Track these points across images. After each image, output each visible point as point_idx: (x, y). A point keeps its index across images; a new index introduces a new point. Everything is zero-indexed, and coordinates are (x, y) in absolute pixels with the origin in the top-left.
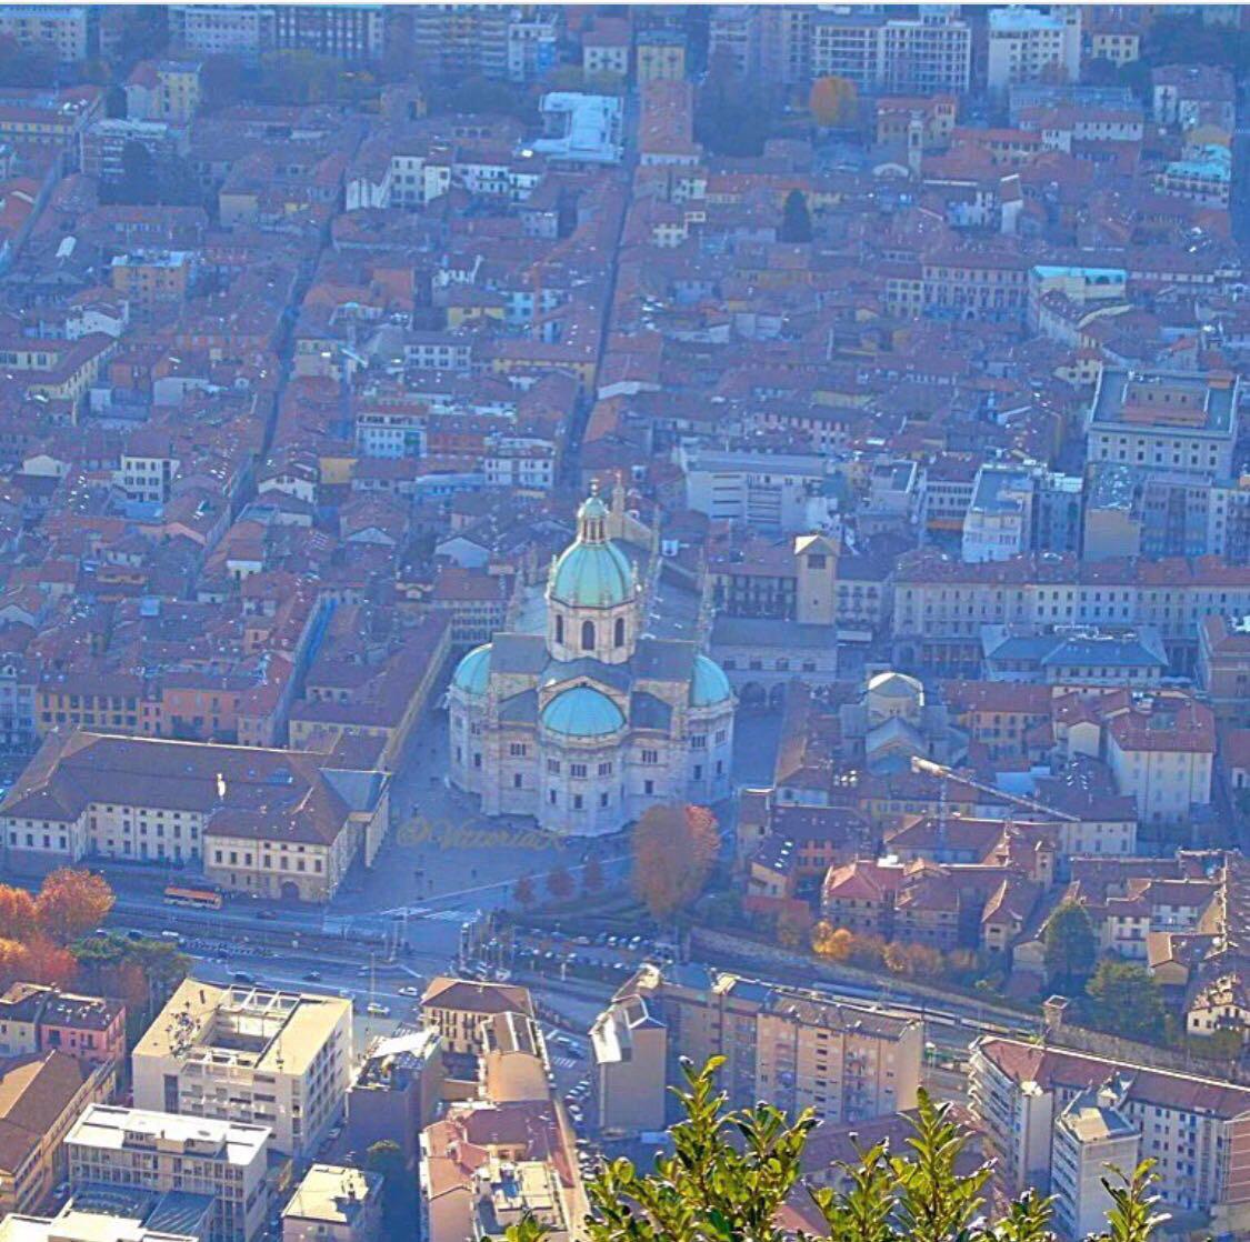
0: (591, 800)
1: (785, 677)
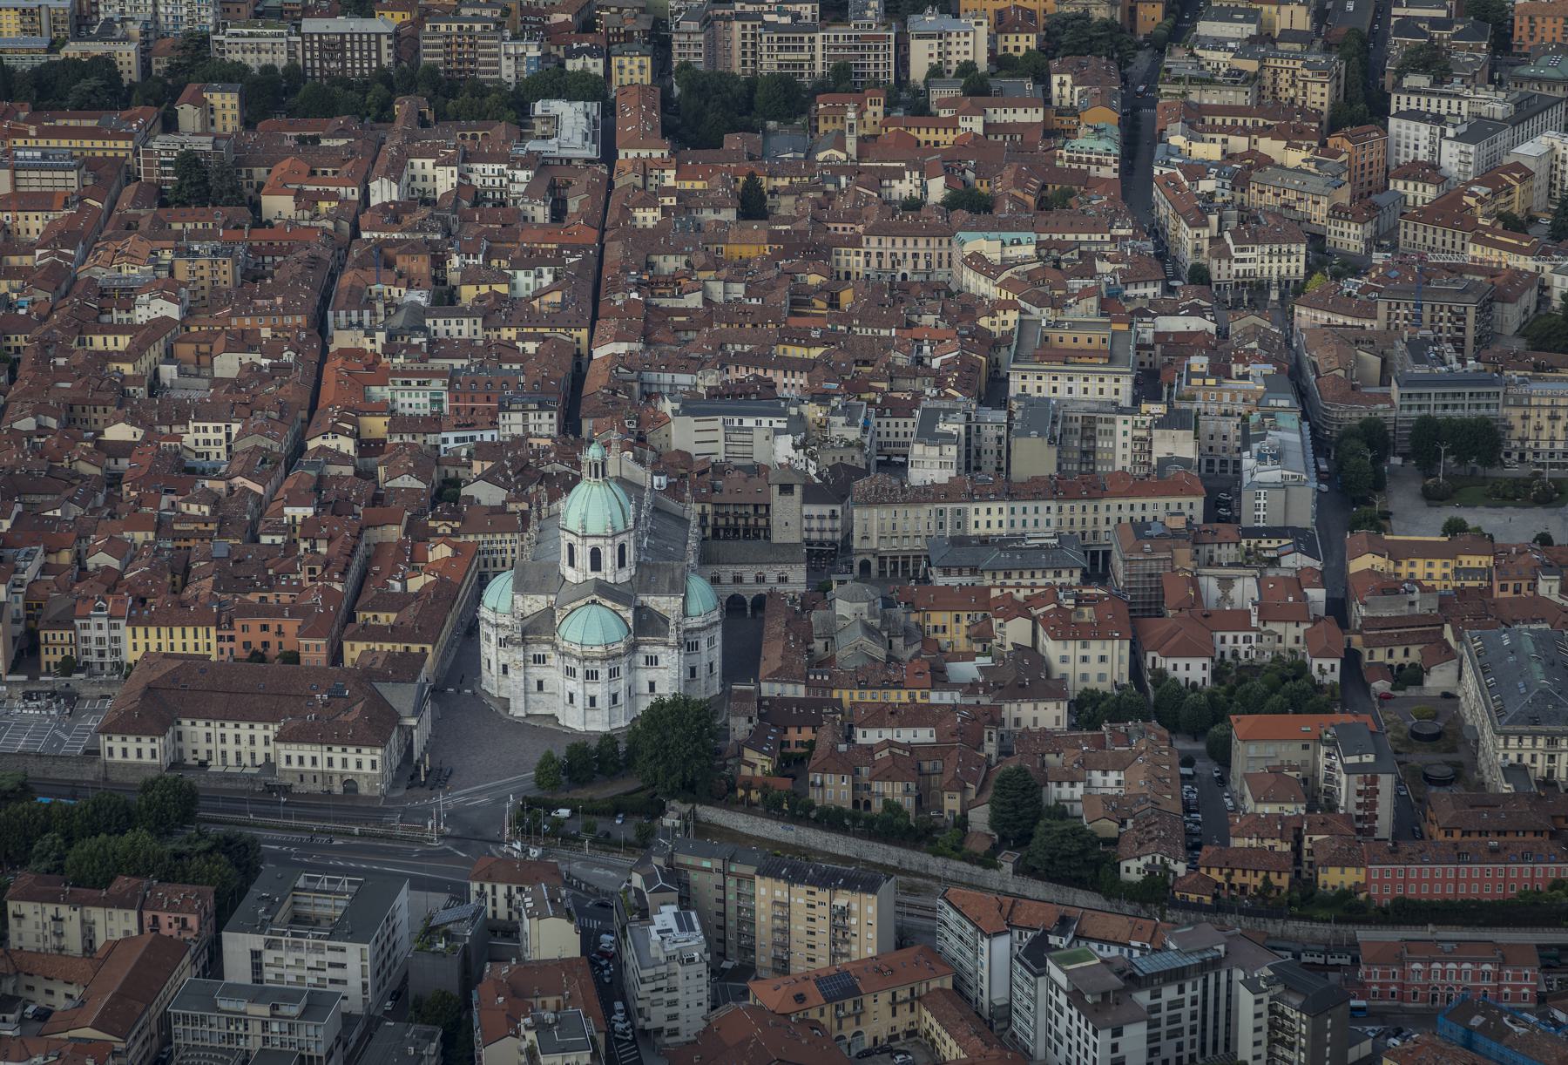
0: (603, 701)
1: (763, 589)
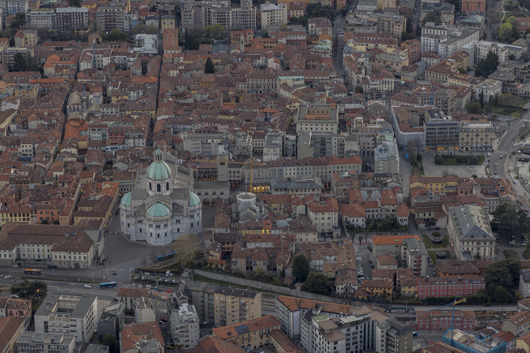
0: (162, 235)
1: (215, 197)
